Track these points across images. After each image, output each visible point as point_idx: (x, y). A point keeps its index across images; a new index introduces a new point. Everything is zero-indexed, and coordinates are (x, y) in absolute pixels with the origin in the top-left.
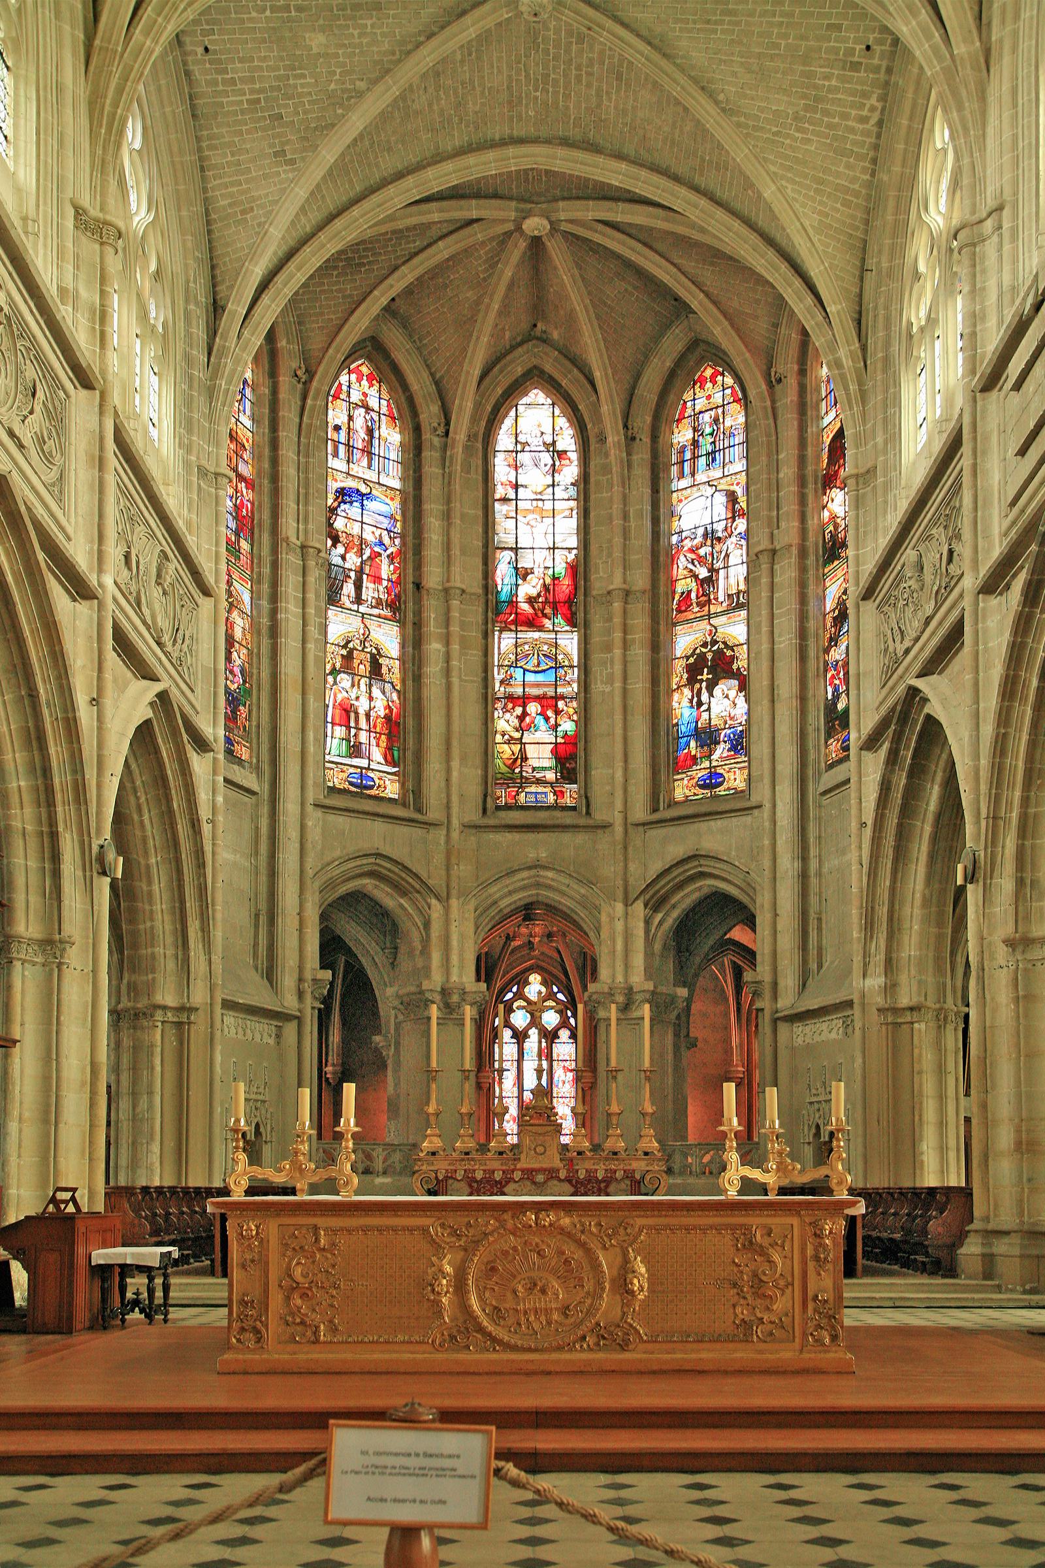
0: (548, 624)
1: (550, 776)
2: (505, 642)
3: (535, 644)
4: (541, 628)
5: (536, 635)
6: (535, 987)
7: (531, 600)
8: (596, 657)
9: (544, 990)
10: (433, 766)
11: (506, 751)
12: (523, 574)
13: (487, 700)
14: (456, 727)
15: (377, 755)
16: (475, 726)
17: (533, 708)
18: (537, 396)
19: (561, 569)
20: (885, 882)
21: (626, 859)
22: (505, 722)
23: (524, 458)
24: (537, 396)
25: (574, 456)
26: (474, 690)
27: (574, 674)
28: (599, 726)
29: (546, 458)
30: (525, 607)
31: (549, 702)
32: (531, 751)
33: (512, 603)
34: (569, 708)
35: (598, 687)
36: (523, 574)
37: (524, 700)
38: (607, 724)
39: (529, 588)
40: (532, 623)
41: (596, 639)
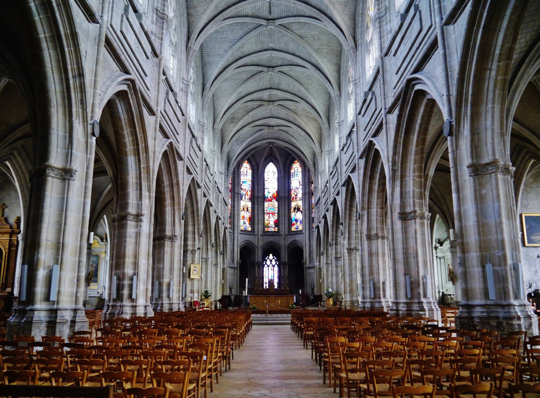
0: (273, 201)
1: (273, 226)
2: (266, 204)
3: (271, 204)
4: (272, 202)
5: (271, 203)
6: (271, 256)
7: (270, 197)
8: (280, 207)
9: (272, 257)
10: (256, 225)
11: (266, 222)
12: (269, 193)
13: (264, 214)
14: (259, 219)
15: (247, 223)
16: (262, 219)
17: (271, 215)
18: (271, 164)
19: (275, 192)
20: (318, 249)
21: (284, 241)
22: (266, 217)
23: (269, 174)
24: (271, 164)
25: (277, 173)
26: (262, 212)
27: (277, 209)
28: (280, 219)
29: (273, 174)
30: (269, 198)
31: (273, 214)
32: (270, 222)
33: (268, 198)
34: (276, 215)
35: (280, 212)
36: (269, 193)
37: (269, 214)
38: (282, 218)
39: (270, 195)
40: (271, 201)
41: (280, 204)
